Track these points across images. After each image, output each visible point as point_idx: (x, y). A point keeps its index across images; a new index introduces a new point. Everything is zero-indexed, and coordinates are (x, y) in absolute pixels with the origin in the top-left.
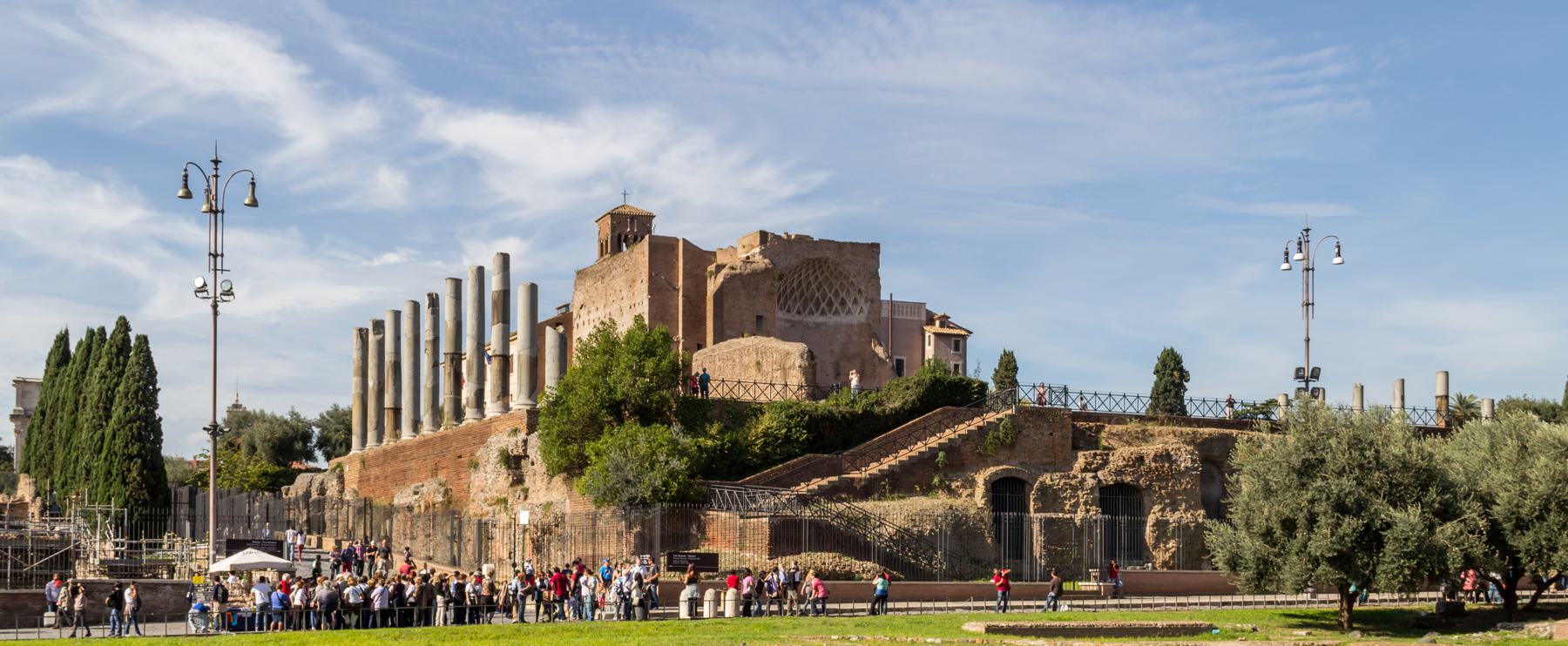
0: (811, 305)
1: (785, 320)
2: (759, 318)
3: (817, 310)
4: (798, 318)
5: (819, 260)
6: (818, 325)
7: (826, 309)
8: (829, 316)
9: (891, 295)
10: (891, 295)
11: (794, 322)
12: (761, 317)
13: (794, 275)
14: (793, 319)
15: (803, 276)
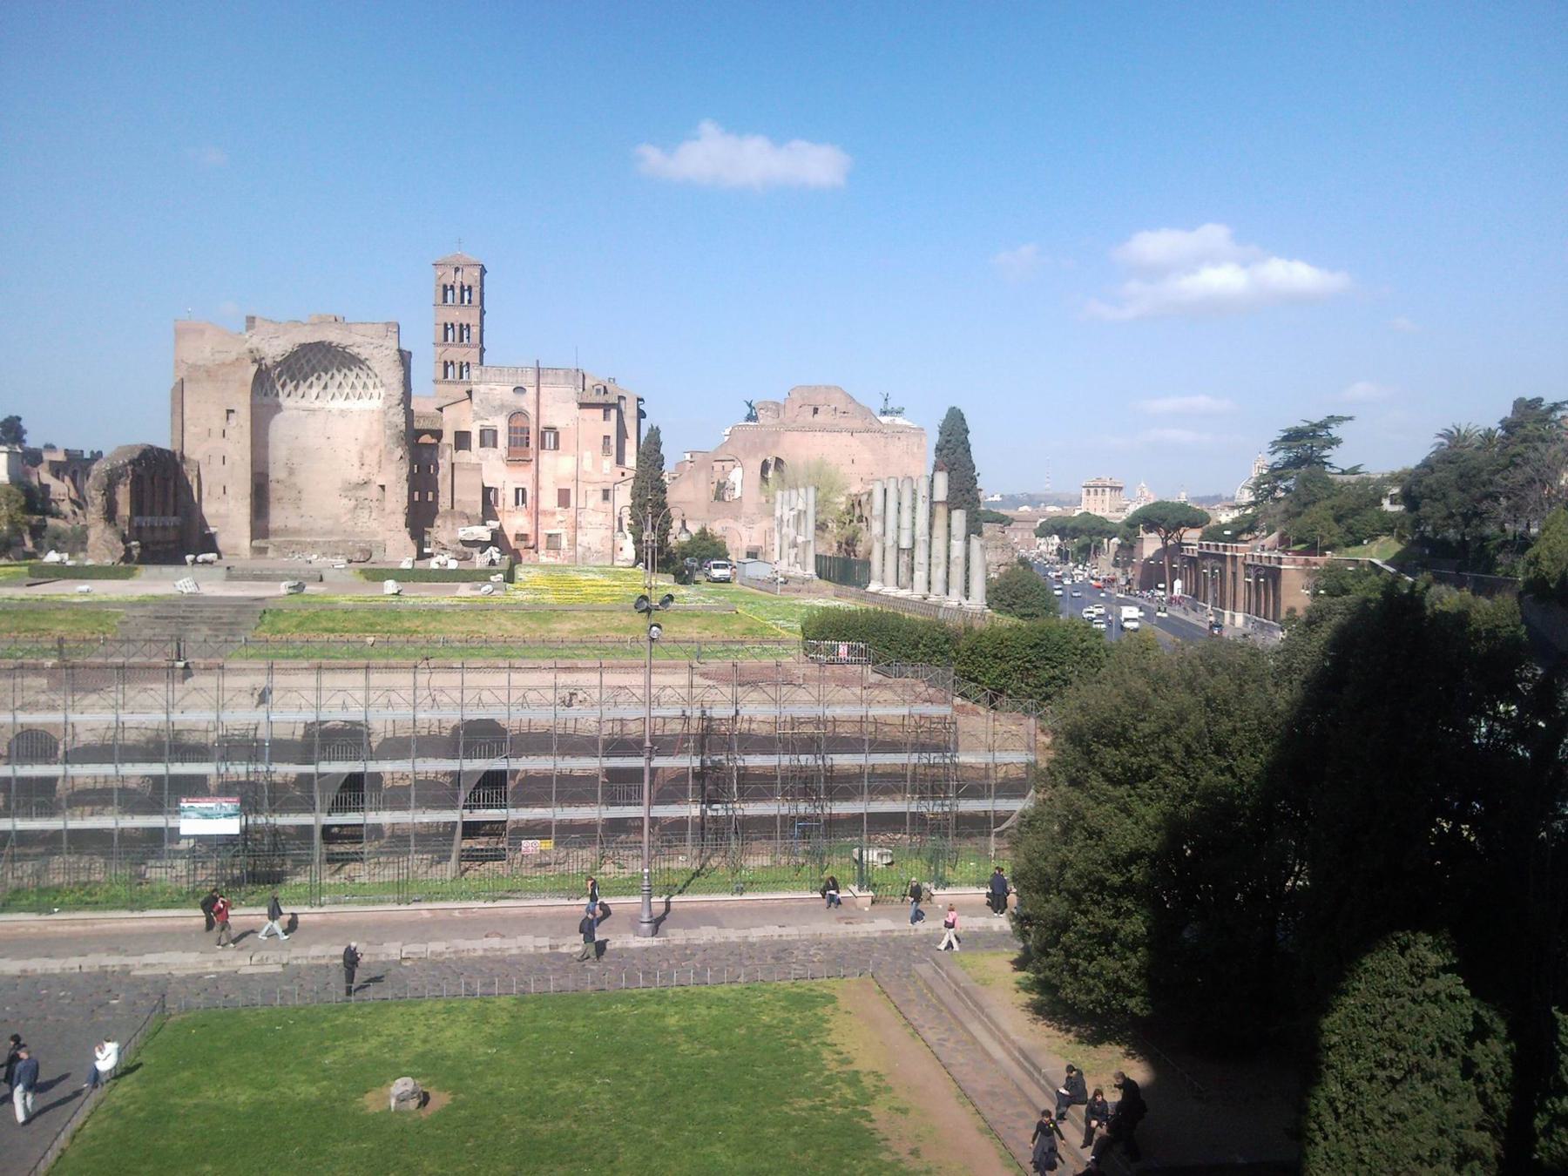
0: (335, 390)
1: (296, 409)
2: (230, 411)
3: (341, 395)
4: (318, 404)
5: (320, 344)
6: (343, 413)
7: (351, 394)
8: (355, 400)
9: (538, 362)
10: (538, 362)
11: (314, 410)
12: (233, 411)
13: (298, 360)
14: (312, 406)
15: (314, 362)
